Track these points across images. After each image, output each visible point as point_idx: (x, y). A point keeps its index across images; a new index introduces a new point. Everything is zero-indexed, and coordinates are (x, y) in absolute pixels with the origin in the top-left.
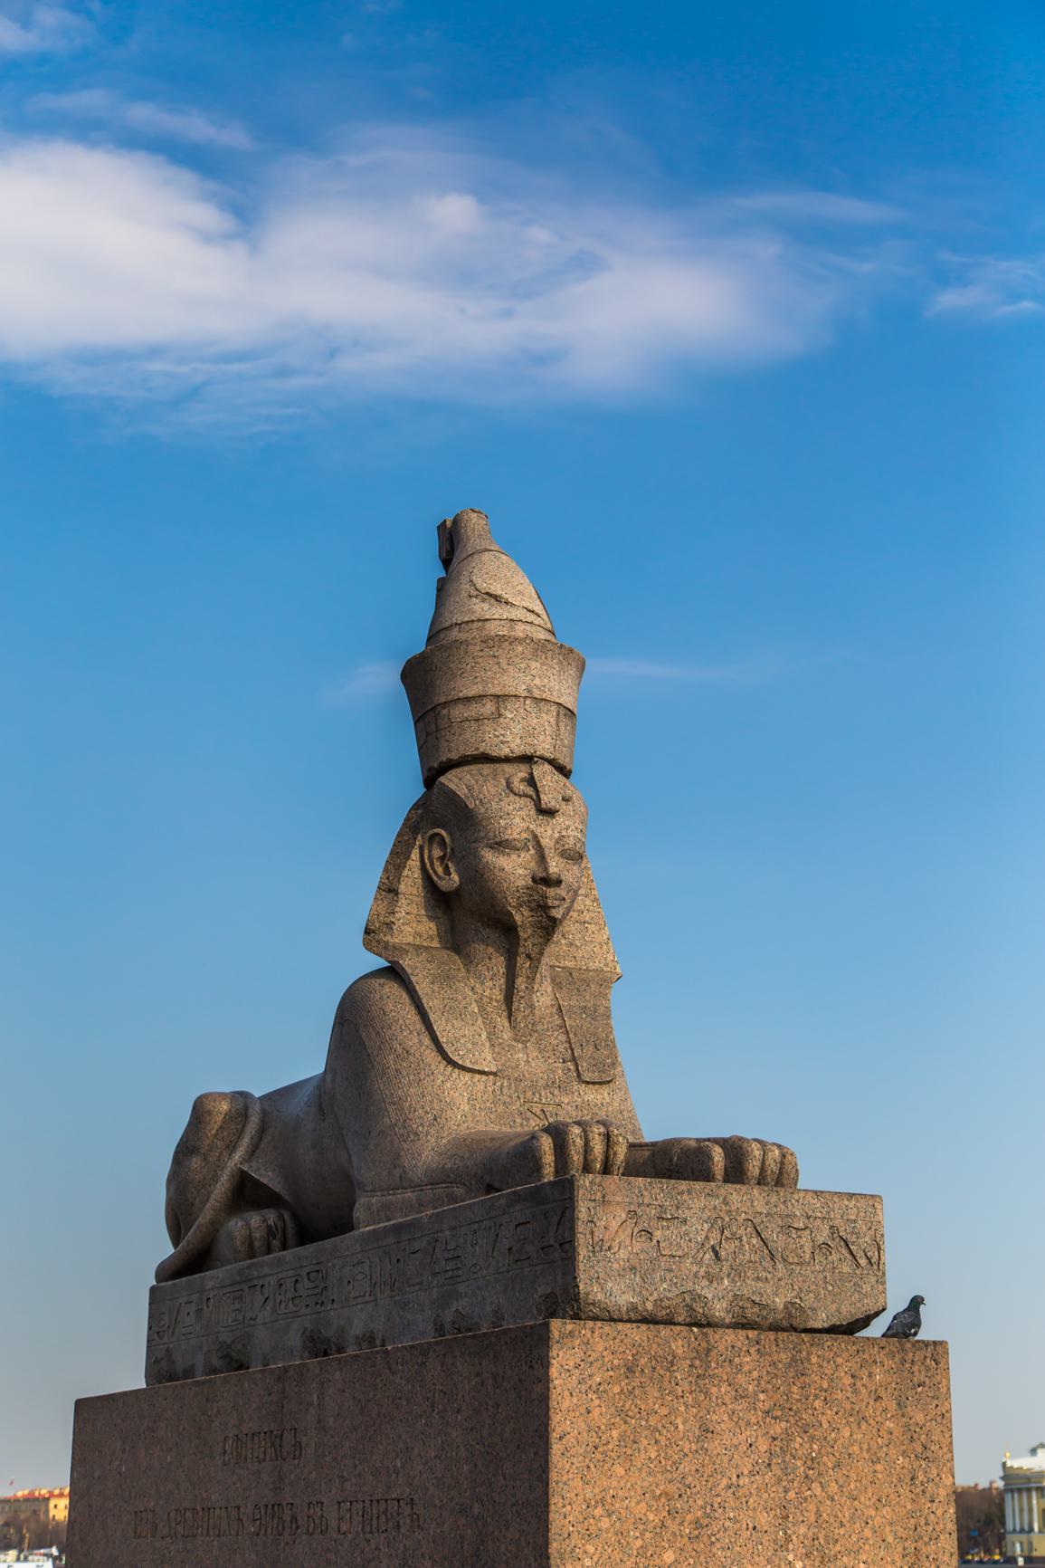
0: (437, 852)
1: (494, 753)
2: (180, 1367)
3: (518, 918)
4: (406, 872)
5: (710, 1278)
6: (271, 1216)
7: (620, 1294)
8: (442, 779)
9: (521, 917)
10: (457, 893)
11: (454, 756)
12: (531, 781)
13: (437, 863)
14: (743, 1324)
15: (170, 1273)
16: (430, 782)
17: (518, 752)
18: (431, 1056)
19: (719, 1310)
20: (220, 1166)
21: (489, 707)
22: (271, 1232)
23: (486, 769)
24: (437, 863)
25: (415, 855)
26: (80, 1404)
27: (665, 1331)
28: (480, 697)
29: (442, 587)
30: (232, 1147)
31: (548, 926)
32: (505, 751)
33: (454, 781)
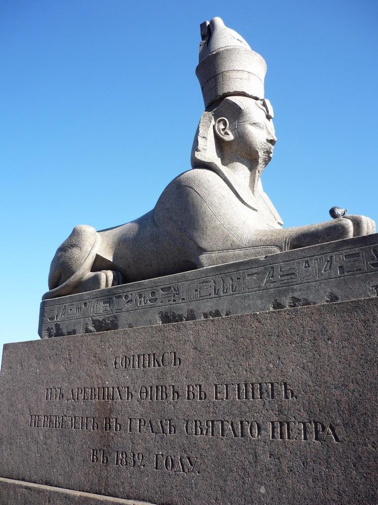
0: (222, 126)
1: (247, 92)
2: (65, 331)
3: (259, 153)
4: (209, 132)
8: (228, 98)
9: (261, 154)
10: (230, 143)
11: (231, 91)
13: (222, 132)
15: (46, 296)
17: (254, 95)
24: (222, 132)
25: (211, 127)
26: (6, 347)
31: (267, 161)
32: (250, 93)
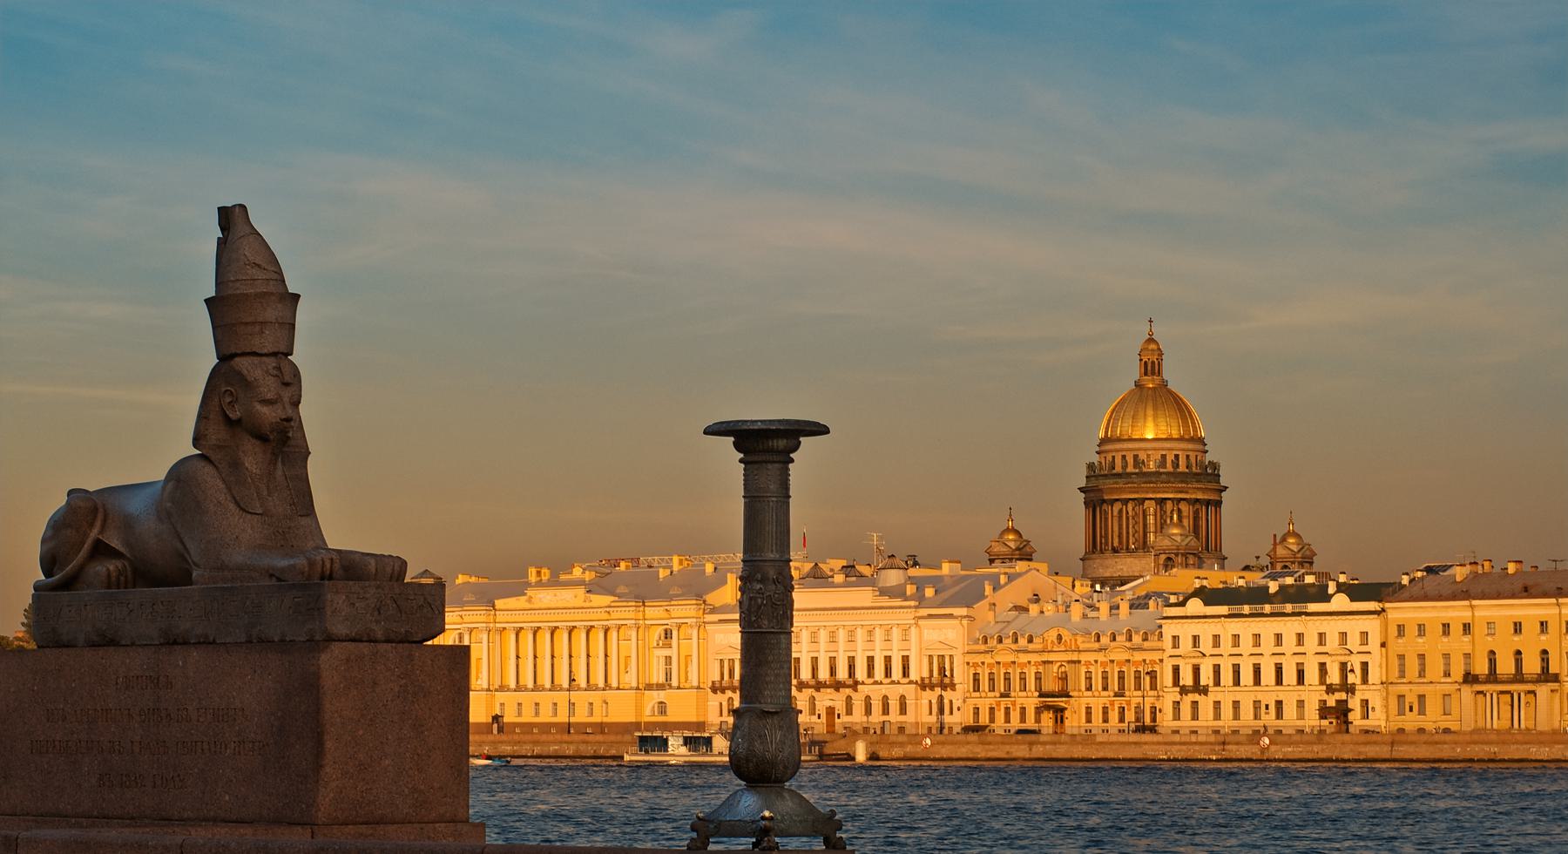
5: (377, 622)
6: (119, 564)
7: (340, 629)
10: (239, 421)
12: (279, 368)
14: (388, 641)
16: (224, 358)
18: (232, 506)
19: (380, 635)
20: (86, 535)
21: (257, 328)
22: (120, 573)
23: (256, 360)
27: (361, 645)
28: (253, 323)
29: (222, 243)
30: (92, 525)
33: (242, 364)
